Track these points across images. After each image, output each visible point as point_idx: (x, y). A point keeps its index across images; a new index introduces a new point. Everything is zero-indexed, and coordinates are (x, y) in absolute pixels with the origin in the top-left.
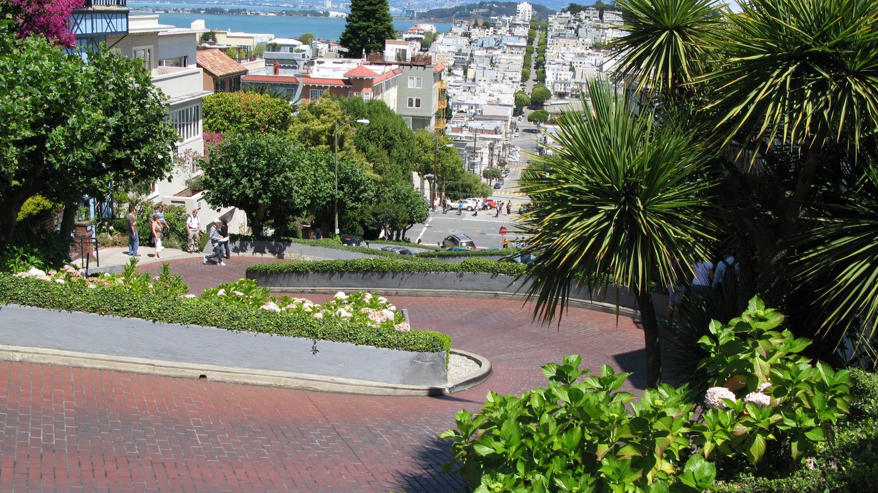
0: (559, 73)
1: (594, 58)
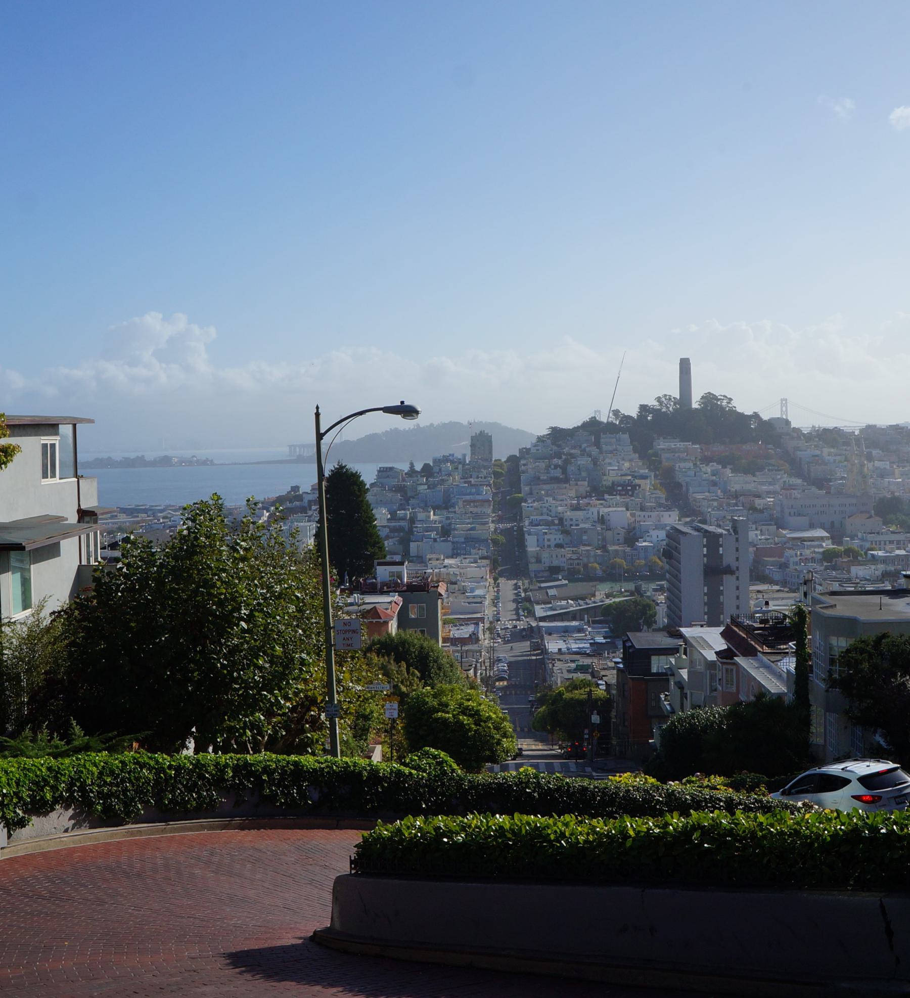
0: (546, 537)
1: (595, 510)
